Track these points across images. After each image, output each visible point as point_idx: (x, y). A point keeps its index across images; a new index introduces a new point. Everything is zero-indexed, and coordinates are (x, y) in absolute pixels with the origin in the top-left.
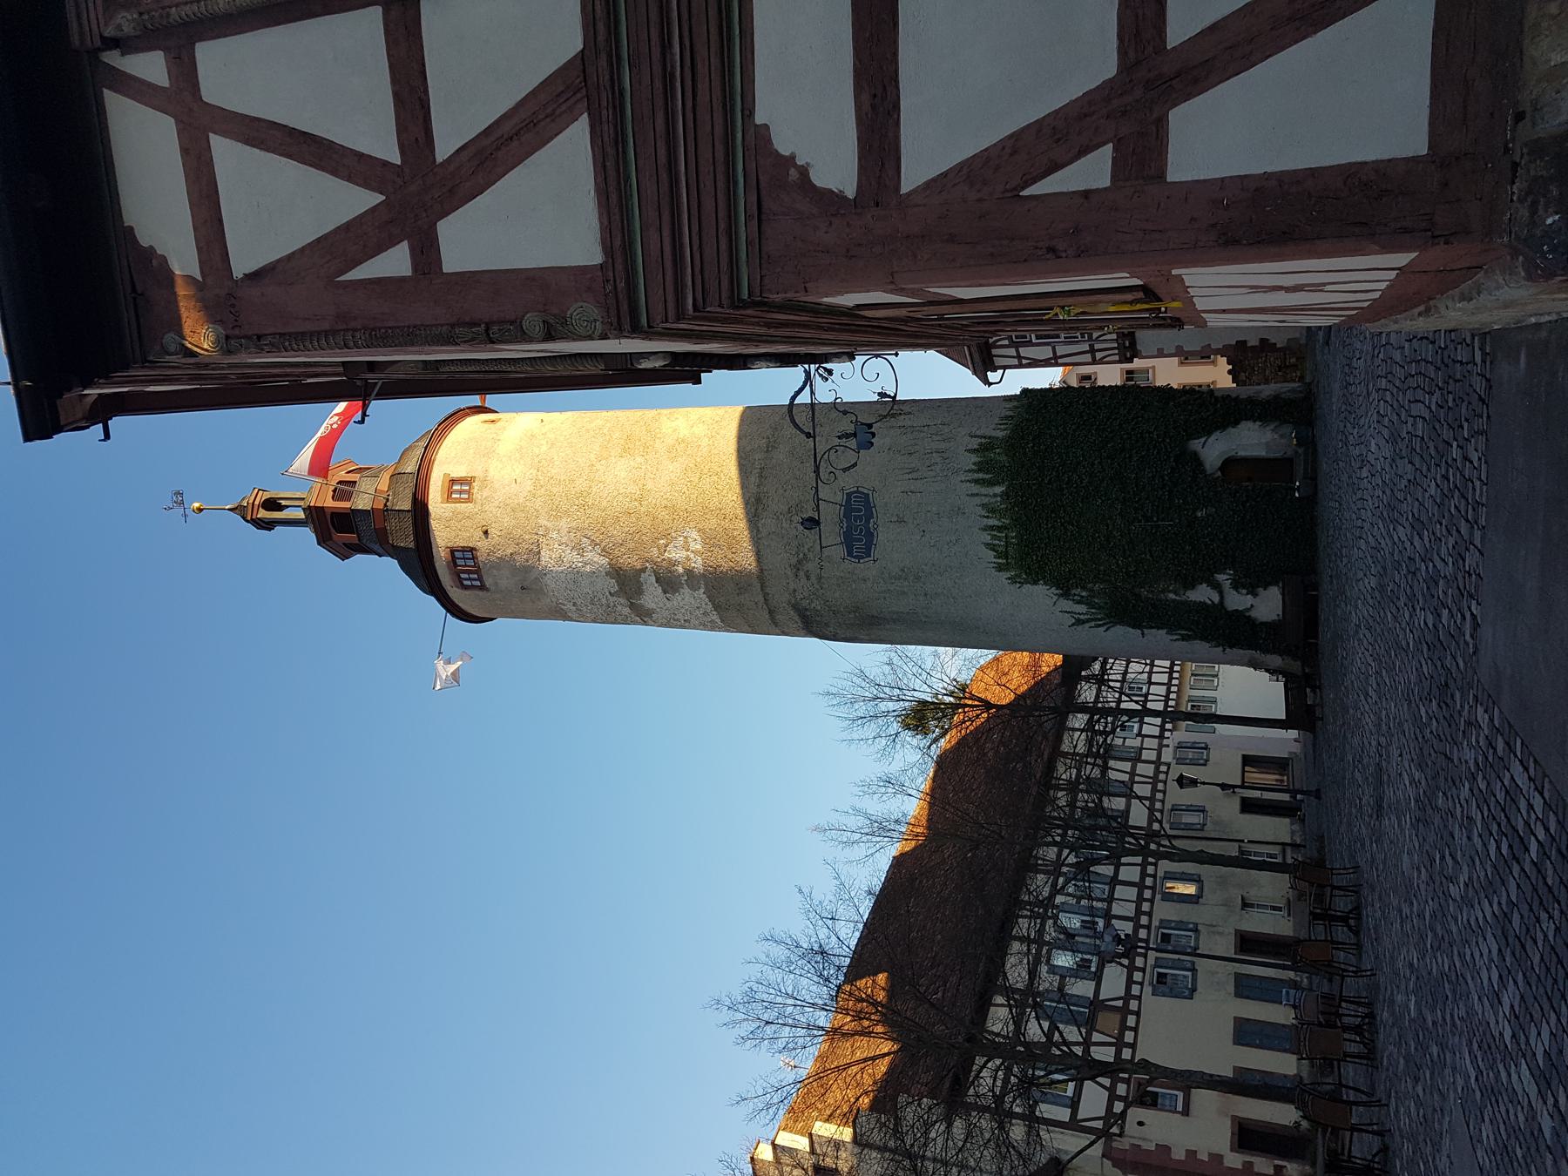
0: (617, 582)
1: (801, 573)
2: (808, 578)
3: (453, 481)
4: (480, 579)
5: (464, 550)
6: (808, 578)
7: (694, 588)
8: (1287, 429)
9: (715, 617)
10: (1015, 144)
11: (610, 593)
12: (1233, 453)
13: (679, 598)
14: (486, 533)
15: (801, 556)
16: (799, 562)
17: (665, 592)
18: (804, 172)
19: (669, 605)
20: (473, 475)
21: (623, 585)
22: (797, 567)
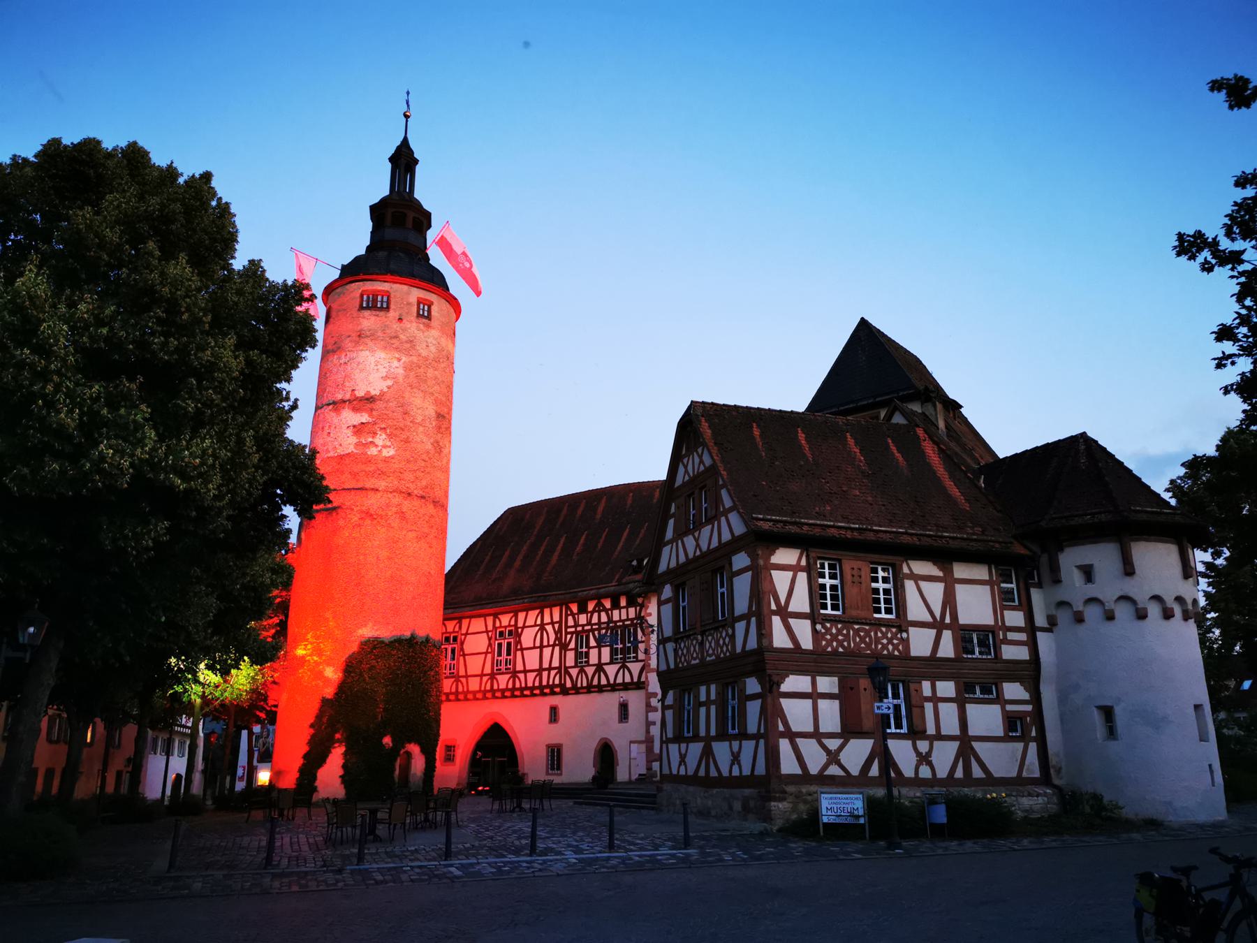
0: (363, 397)
1: (363, 515)
2: (362, 519)
3: (429, 307)
4: (368, 308)
5: (388, 302)
6: (362, 519)
7: (357, 445)
8: (421, 784)
9: (331, 454)
10: (785, 717)
11: (354, 390)
12: (413, 757)
13: (349, 435)
14: (400, 320)
15: (375, 517)
16: (371, 515)
17: (354, 426)
18: (783, 683)
19: (344, 427)
20: (432, 320)
21: (361, 400)
22: (368, 514)
